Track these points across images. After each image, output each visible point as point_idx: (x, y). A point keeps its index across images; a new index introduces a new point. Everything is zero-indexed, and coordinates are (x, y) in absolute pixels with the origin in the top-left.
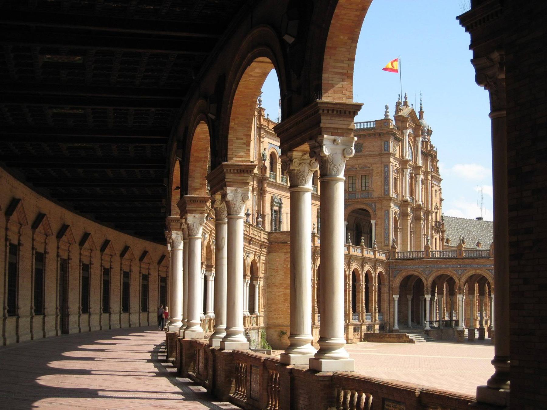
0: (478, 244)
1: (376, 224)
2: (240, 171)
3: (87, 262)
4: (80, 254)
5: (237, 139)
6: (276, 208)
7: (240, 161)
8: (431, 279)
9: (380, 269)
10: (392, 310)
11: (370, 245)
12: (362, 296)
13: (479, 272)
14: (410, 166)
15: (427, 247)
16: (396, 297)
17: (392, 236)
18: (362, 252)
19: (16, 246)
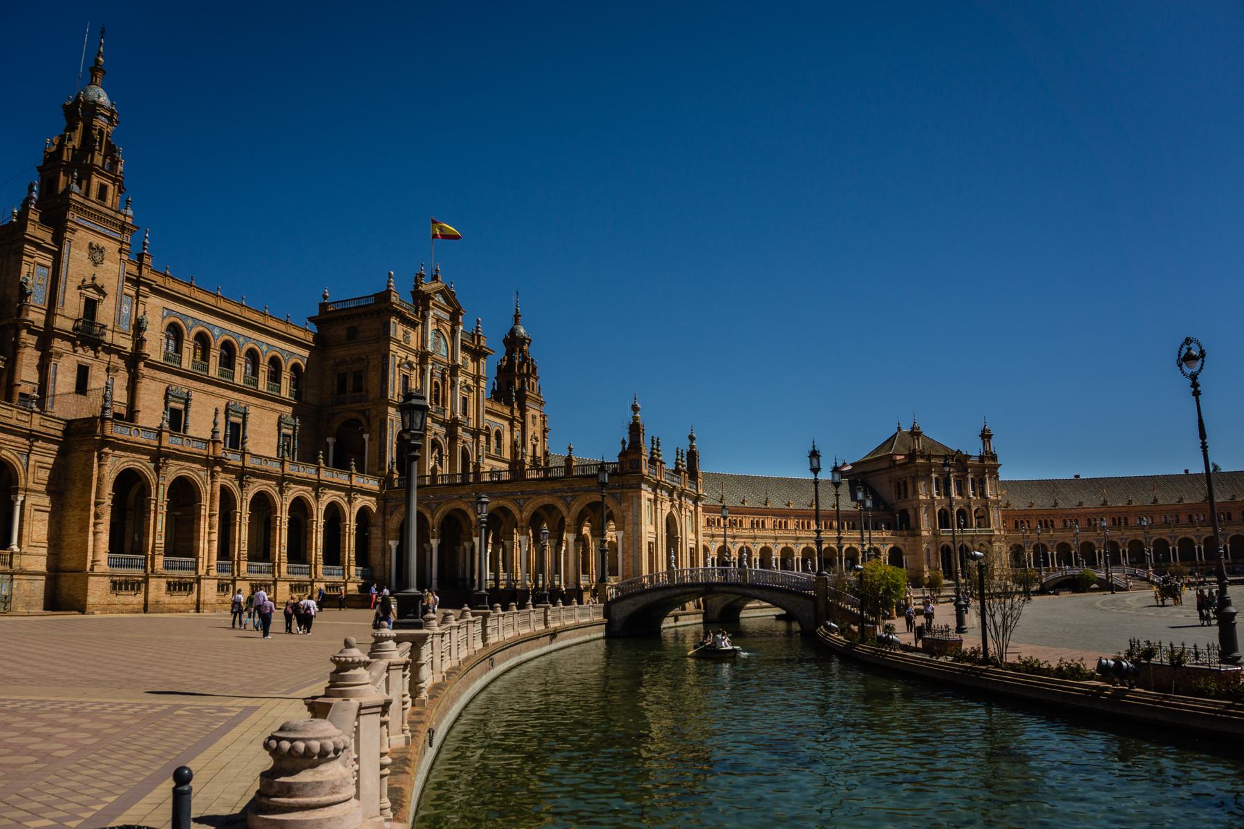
1: (370, 439)
8: (438, 516)
9: (360, 501)
10: (387, 563)
11: (361, 470)
13: (502, 502)
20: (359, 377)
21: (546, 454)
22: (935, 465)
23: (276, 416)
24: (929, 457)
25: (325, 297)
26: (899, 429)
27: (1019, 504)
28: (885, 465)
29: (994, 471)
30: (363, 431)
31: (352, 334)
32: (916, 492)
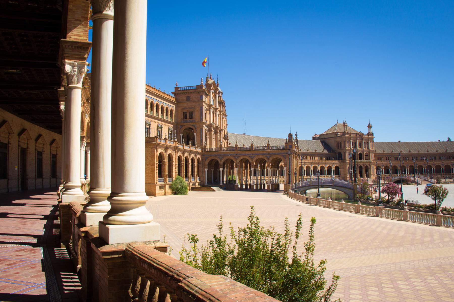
0: (244, 145)
2: (78, 47)
3: (40, 150)
4: (36, 146)
5: (76, 20)
6: (148, 127)
7: (79, 39)
8: (223, 161)
9: (198, 156)
11: (193, 145)
12: (190, 169)
13: (245, 157)
14: (213, 107)
15: (221, 146)
16: (206, 170)
17: (204, 141)
18: (190, 148)
19: (6, 144)
20: (192, 114)
21: (227, 134)
22: (352, 137)
23: (167, 128)
24: (350, 134)
25: (177, 85)
26: (338, 122)
27: (379, 151)
28: (333, 136)
29: (372, 140)
30: (193, 132)
31: (188, 99)
32: (345, 146)
